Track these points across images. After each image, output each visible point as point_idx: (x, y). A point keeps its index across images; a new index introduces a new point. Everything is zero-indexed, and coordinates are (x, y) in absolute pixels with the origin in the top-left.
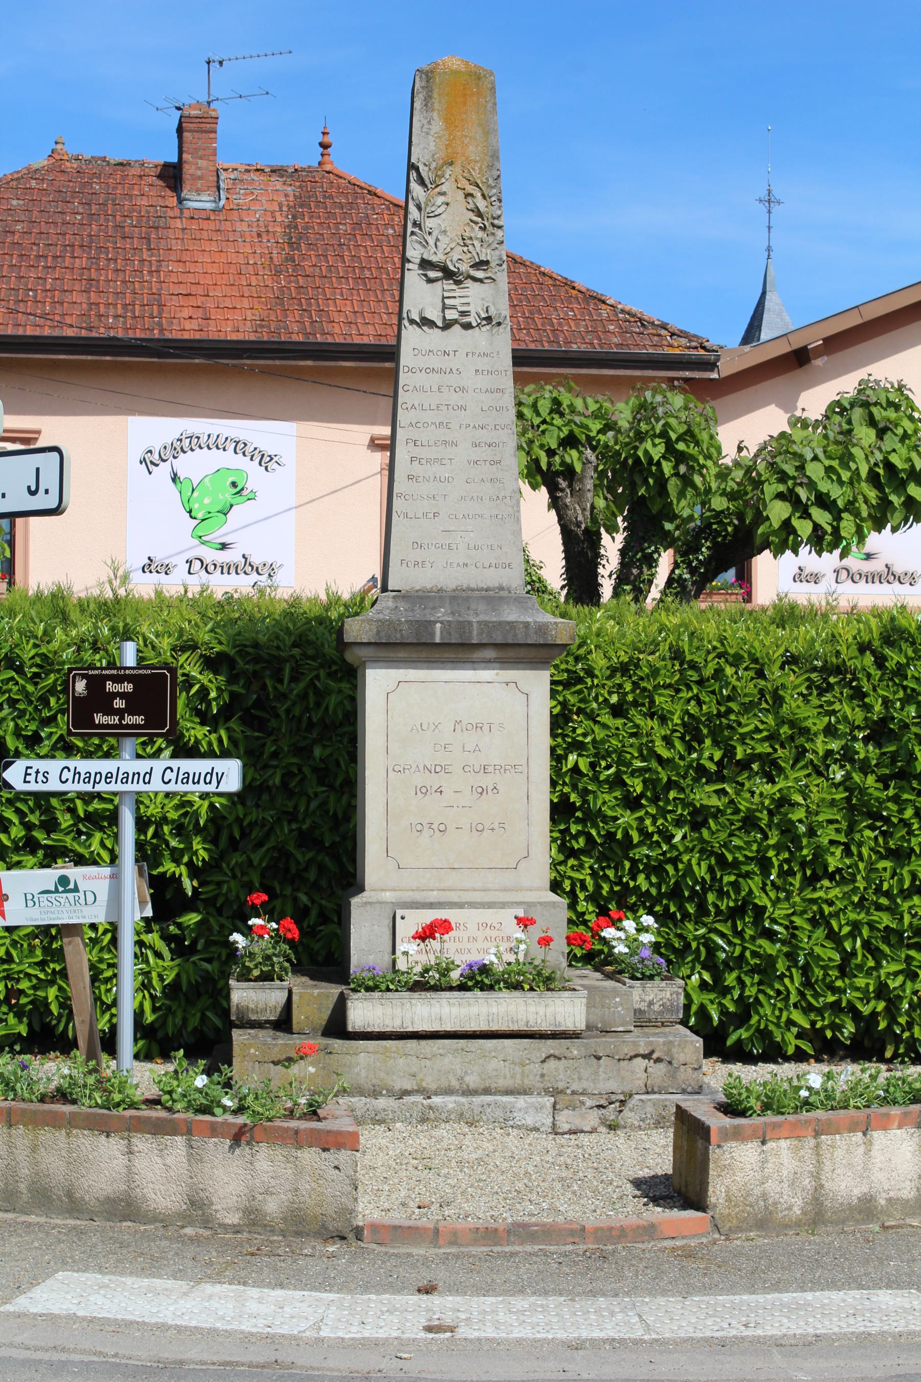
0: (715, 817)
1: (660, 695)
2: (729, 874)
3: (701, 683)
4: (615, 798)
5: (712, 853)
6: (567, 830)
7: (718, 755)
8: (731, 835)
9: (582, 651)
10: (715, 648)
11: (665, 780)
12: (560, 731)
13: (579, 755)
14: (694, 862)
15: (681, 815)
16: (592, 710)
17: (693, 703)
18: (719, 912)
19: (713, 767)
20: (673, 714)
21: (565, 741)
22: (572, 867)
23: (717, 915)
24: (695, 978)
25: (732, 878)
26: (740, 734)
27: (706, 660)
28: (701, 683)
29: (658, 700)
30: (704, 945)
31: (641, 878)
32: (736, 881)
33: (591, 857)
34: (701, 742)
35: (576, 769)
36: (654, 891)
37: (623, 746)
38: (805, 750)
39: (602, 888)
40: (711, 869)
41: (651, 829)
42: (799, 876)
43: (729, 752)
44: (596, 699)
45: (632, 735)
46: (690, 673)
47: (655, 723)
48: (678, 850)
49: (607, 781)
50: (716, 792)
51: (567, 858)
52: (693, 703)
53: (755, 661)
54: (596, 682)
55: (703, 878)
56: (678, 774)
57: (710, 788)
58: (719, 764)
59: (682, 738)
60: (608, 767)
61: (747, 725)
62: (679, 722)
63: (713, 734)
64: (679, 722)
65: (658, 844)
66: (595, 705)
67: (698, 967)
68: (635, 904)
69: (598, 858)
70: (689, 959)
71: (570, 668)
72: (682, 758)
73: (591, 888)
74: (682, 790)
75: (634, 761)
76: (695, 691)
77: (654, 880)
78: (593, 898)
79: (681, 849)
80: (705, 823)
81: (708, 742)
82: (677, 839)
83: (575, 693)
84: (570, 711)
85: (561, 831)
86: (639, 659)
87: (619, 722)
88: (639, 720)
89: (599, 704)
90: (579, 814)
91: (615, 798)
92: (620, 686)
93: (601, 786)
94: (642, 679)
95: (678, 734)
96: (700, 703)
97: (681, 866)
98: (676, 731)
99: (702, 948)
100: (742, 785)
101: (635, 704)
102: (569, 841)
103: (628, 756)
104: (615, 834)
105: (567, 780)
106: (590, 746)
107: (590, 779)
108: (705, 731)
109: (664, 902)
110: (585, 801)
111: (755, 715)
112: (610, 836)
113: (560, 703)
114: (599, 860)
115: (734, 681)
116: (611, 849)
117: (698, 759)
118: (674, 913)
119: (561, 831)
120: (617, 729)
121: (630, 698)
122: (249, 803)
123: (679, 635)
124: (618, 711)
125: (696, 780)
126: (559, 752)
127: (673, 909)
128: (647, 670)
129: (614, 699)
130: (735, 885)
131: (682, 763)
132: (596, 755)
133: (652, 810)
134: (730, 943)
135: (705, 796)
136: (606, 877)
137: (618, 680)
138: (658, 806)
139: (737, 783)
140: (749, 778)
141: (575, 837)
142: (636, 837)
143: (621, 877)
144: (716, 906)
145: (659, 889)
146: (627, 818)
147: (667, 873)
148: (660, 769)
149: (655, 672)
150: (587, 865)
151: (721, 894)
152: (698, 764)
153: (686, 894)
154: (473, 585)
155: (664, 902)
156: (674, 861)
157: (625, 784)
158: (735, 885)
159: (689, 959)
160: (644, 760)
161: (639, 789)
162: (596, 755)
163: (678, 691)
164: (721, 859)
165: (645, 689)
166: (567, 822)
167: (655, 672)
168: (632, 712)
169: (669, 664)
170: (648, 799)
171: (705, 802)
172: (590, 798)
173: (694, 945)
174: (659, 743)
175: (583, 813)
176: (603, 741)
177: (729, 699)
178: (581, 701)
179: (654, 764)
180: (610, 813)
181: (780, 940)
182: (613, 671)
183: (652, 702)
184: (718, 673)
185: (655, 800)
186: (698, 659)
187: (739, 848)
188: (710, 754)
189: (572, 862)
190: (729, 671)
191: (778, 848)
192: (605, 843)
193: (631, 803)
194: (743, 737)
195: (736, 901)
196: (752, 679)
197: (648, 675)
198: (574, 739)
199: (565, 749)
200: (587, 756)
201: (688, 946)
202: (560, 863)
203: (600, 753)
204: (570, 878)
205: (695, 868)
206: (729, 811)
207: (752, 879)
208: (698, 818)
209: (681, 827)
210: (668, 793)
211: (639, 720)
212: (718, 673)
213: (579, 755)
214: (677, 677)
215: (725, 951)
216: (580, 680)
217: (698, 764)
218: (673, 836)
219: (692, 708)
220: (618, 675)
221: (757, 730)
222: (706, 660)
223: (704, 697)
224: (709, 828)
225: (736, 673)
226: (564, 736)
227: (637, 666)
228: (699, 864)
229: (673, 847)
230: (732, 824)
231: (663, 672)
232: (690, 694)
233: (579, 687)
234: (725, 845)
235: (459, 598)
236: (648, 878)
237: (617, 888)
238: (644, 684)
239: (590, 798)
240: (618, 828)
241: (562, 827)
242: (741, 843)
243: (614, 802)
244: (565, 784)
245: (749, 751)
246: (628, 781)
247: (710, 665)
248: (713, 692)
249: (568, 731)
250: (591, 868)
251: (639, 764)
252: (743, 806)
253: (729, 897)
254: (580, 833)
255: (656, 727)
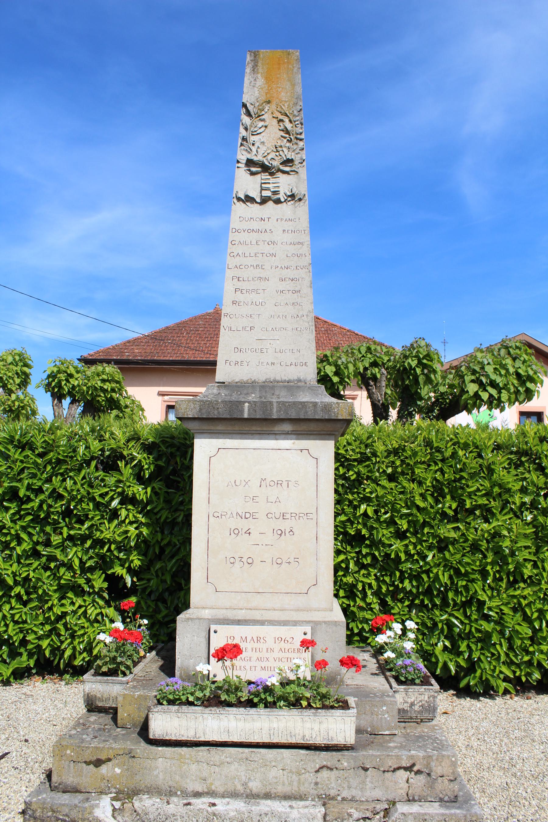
0: (453, 544)
1: (418, 468)
2: (462, 580)
3: (443, 460)
4: (390, 532)
5: (451, 567)
6: (360, 551)
7: (454, 506)
8: (463, 555)
9: (370, 441)
10: (451, 439)
11: (422, 521)
12: (356, 490)
13: (368, 505)
14: (440, 573)
15: (432, 543)
16: (376, 477)
17: (438, 473)
18: (455, 604)
19: (451, 513)
20: (426, 480)
21: (359, 497)
22: (363, 575)
23: (454, 606)
24: (440, 645)
25: (464, 583)
26: (468, 492)
27: (446, 447)
28: (443, 460)
29: (417, 471)
30: (446, 624)
31: (407, 583)
32: (467, 585)
33: (375, 568)
34: (444, 497)
35: (365, 514)
36: (414, 590)
37: (395, 500)
38: (509, 502)
39: (382, 588)
40: (451, 577)
41: (413, 552)
42: (505, 581)
43: (462, 503)
44: (378, 470)
45: (401, 493)
46: (437, 454)
47: (415, 486)
48: (430, 565)
49: (385, 521)
50: (453, 528)
51: (360, 569)
52: (438, 473)
53: (477, 447)
54: (378, 459)
55: (446, 583)
56: (430, 518)
57: (450, 526)
58: (455, 511)
59: (432, 495)
60: (386, 513)
61: (472, 487)
62: (430, 485)
63: (450, 492)
64: (430, 485)
65: (417, 561)
66: (377, 474)
67: (442, 638)
68: (403, 598)
69: (380, 569)
70: (437, 633)
71: (362, 451)
72: (432, 507)
73: (375, 588)
74: (432, 527)
75: (402, 510)
76: (440, 466)
77: (415, 583)
78: (377, 593)
79: (432, 565)
80: (446, 548)
81: (448, 497)
82: (429, 558)
83: (365, 466)
84: (362, 478)
85: (356, 552)
86: (405, 446)
87: (393, 485)
88: (405, 484)
89: (380, 473)
90: (367, 542)
91: (390, 532)
92: (393, 462)
93: (381, 525)
94: (407, 458)
95: (430, 492)
96: (443, 473)
97: (431, 575)
98: (428, 490)
99: (445, 627)
100: (469, 524)
101: (403, 473)
102: (361, 559)
103: (399, 506)
104: (390, 555)
105: (360, 521)
106: (374, 500)
107: (375, 521)
108: (446, 490)
109: (421, 597)
110: (371, 534)
111: (477, 481)
112: (387, 556)
113: (356, 473)
114: (380, 570)
115: (464, 460)
116: (388, 564)
117: (442, 508)
118: (428, 604)
119: (356, 552)
120: (392, 489)
121: (399, 470)
122: (166, 532)
123: (429, 432)
124: (392, 478)
125: (441, 521)
126: (355, 503)
127: (426, 602)
128: (410, 453)
129: (390, 470)
130: (466, 588)
131: (432, 511)
132: (378, 505)
133: (413, 540)
134: (462, 623)
135: (447, 531)
136: (384, 582)
137: (392, 458)
138: (417, 537)
139: (466, 523)
140: (474, 520)
141: (365, 556)
142: (403, 557)
143: (394, 582)
144: (453, 600)
145: (418, 588)
146: (398, 545)
147: (423, 579)
148: (418, 514)
149: (415, 454)
150: (372, 574)
151: (457, 592)
152: (442, 511)
153: (435, 593)
154: (278, 378)
155: (421, 597)
156: (427, 572)
157: (397, 524)
158: (466, 588)
159: (437, 633)
160: (408, 508)
161: (405, 527)
162: (378, 505)
163: (429, 466)
164: (457, 572)
165: (408, 464)
166: (360, 547)
167: (415, 454)
168: (401, 478)
169: (424, 449)
170: (411, 533)
171: (446, 535)
172: (375, 532)
173: (440, 625)
174: (417, 498)
175: (370, 541)
176: (383, 497)
177: (461, 470)
178: (368, 472)
179: (415, 511)
180: (387, 542)
181: (493, 621)
182: (389, 453)
183: (413, 473)
184: (454, 455)
185: (415, 533)
186: (442, 445)
187: (468, 564)
188: (449, 504)
189: (363, 572)
190: (461, 453)
191: (493, 563)
192: (384, 560)
193: (401, 535)
194: (470, 495)
195: (466, 597)
196: (475, 458)
197: (410, 456)
198: (364, 495)
199: (359, 501)
200: (373, 506)
201: (435, 624)
202: (356, 572)
203: (380, 504)
204: (362, 582)
205: (441, 577)
206: (461, 540)
207: (476, 583)
208: (443, 545)
209: (431, 551)
210: (423, 529)
211: (405, 484)
212: (454, 455)
213: (368, 505)
214: (429, 457)
215: (459, 627)
216: (368, 459)
217: (442, 511)
218: (427, 556)
219: (438, 476)
220: (392, 456)
221: (478, 490)
222: (446, 447)
223: (446, 469)
224: (449, 551)
225: (465, 455)
226: (358, 493)
227: (404, 450)
228: (443, 575)
229: (427, 563)
230: (464, 549)
231: (420, 454)
232: (437, 468)
233: (367, 463)
234: (460, 562)
235: (268, 386)
236: (411, 582)
237: (391, 589)
238: (408, 461)
239: (375, 532)
240: (392, 551)
241: (357, 550)
242: (469, 561)
243: (389, 535)
244: (358, 523)
245: (474, 503)
246: (398, 522)
247: (449, 450)
248: (451, 466)
249: (361, 490)
250: (375, 575)
251: (405, 511)
252: (471, 537)
253: (462, 594)
254: (367, 554)
255: (416, 488)
